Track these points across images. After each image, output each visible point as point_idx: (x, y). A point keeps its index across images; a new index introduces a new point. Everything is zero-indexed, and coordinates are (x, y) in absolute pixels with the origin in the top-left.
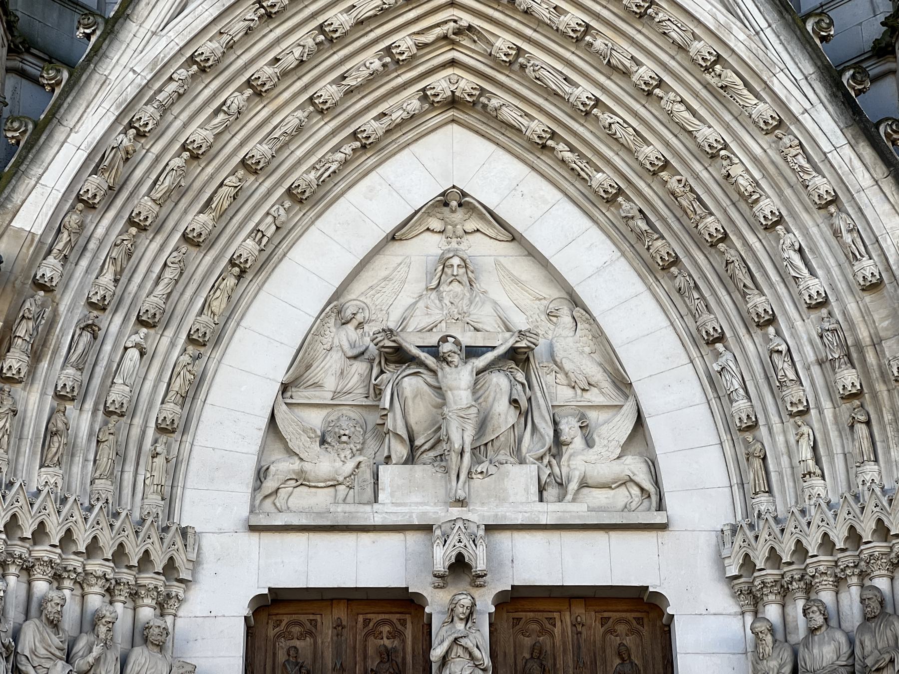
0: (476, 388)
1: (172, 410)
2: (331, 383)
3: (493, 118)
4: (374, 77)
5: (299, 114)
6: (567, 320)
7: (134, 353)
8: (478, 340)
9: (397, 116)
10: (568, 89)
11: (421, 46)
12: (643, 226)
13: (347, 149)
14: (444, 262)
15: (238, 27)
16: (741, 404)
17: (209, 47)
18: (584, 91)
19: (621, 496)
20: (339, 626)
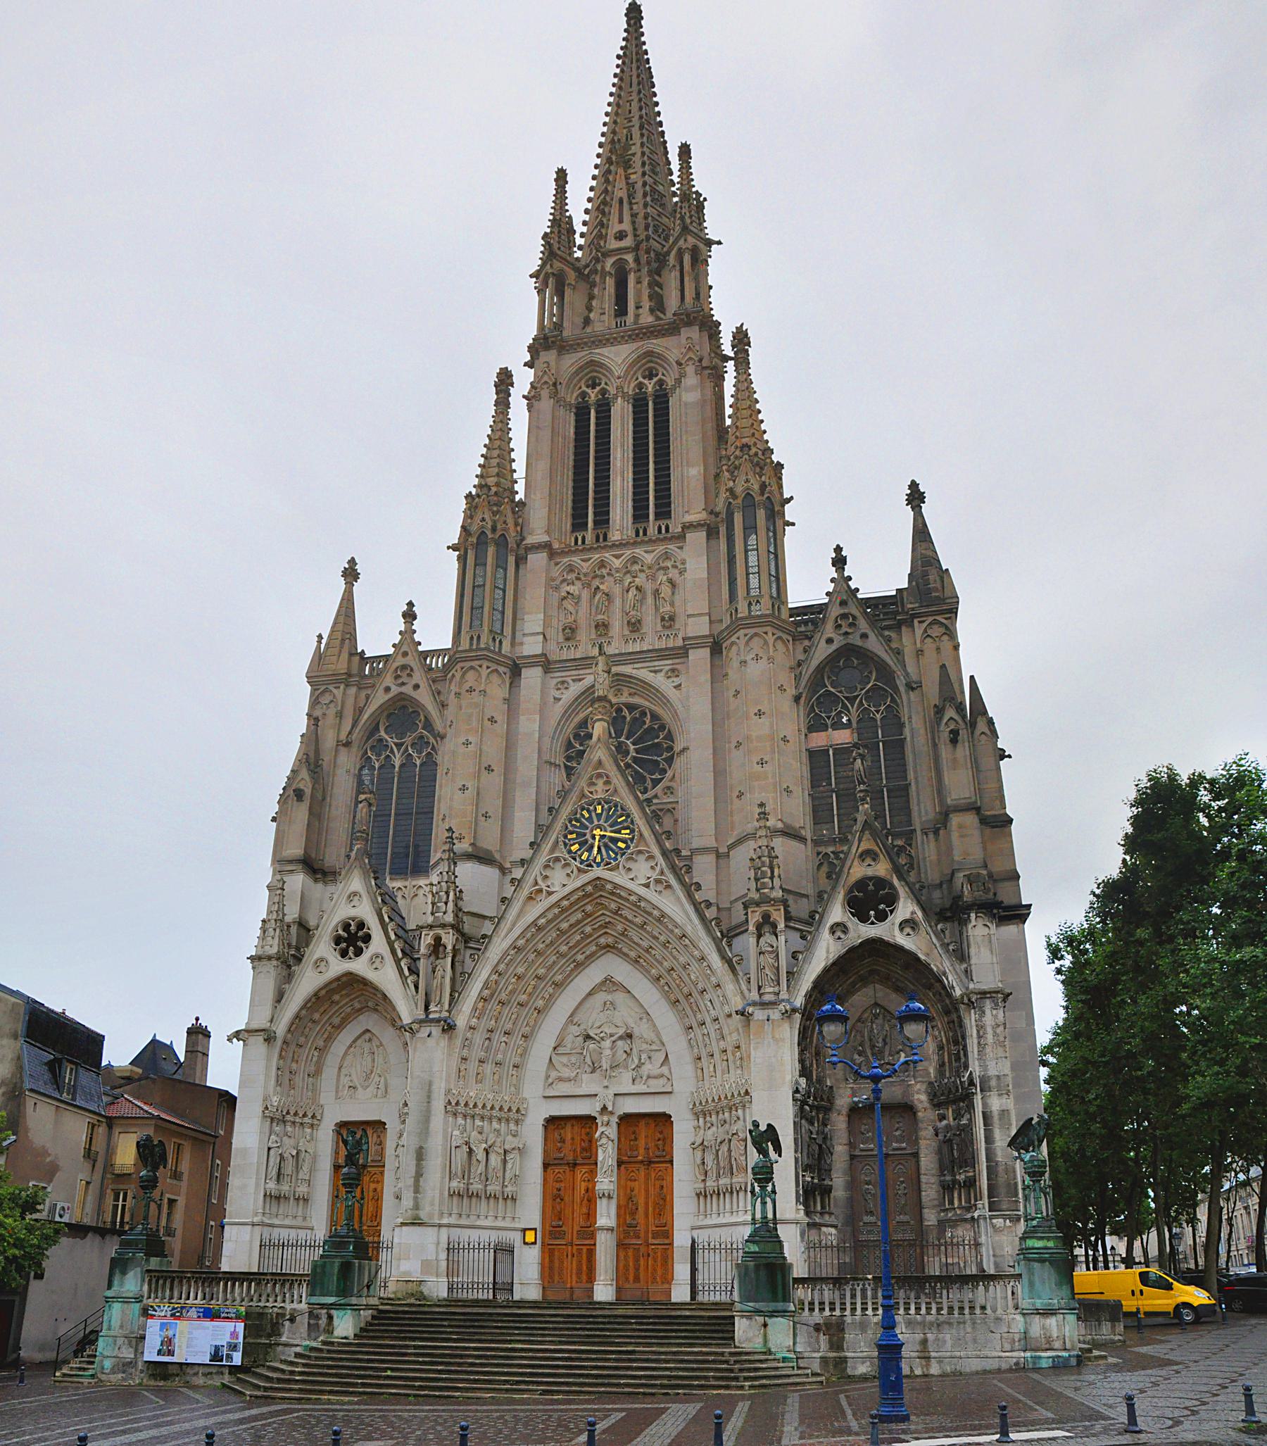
0: (612, 1049)
1: (517, 1060)
2: (569, 1046)
3: (620, 950)
4: (578, 943)
5: (554, 957)
6: (645, 1020)
7: (503, 1044)
8: (613, 1030)
9: (588, 953)
10: (641, 942)
11: (594, 929)
12: (666, 988)
13: (572, 966)
14: (605, 1003)
15: (530, 934)
16: (696, 1050)
17: (521, 942)
18: (645, 944)
19: (662, 1081)
20: (573, 1126)
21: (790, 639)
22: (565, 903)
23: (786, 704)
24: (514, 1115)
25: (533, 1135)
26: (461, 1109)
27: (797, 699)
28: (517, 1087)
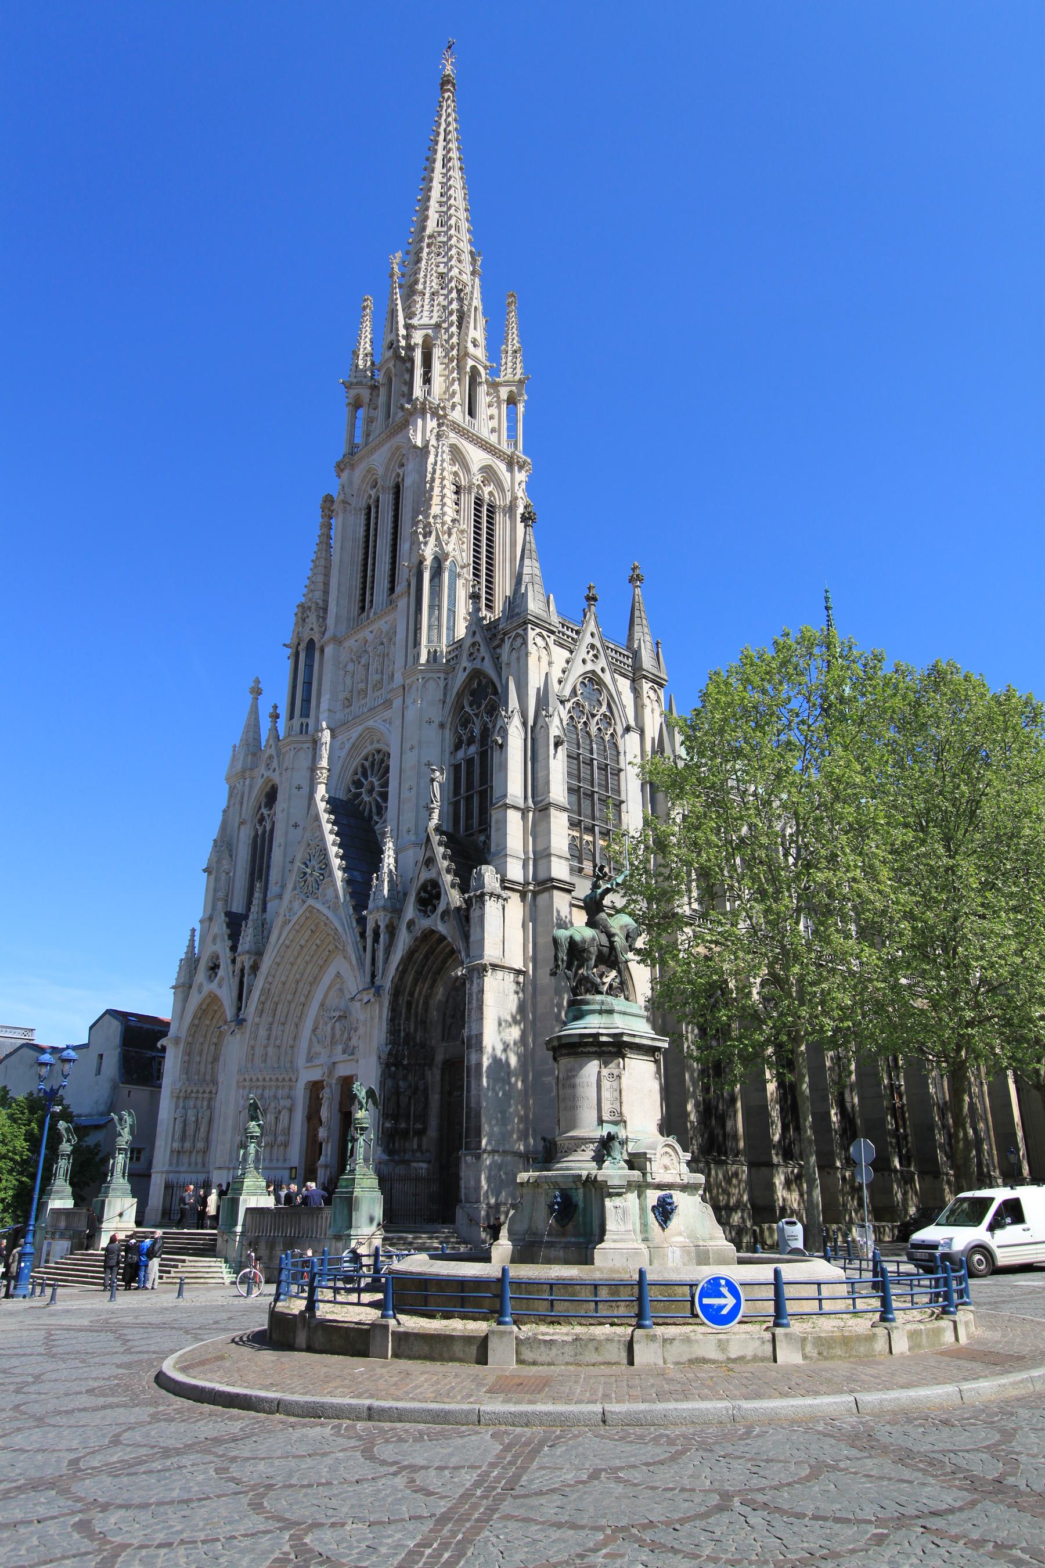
4: (316, 951)
21: (442, 676)
22: (297, 927)
23: (432, 734)
24: (292, 1081)
25: (300, 1093)
26: (247, 1084)
27: (442, 726)
28: (291, 1062)
